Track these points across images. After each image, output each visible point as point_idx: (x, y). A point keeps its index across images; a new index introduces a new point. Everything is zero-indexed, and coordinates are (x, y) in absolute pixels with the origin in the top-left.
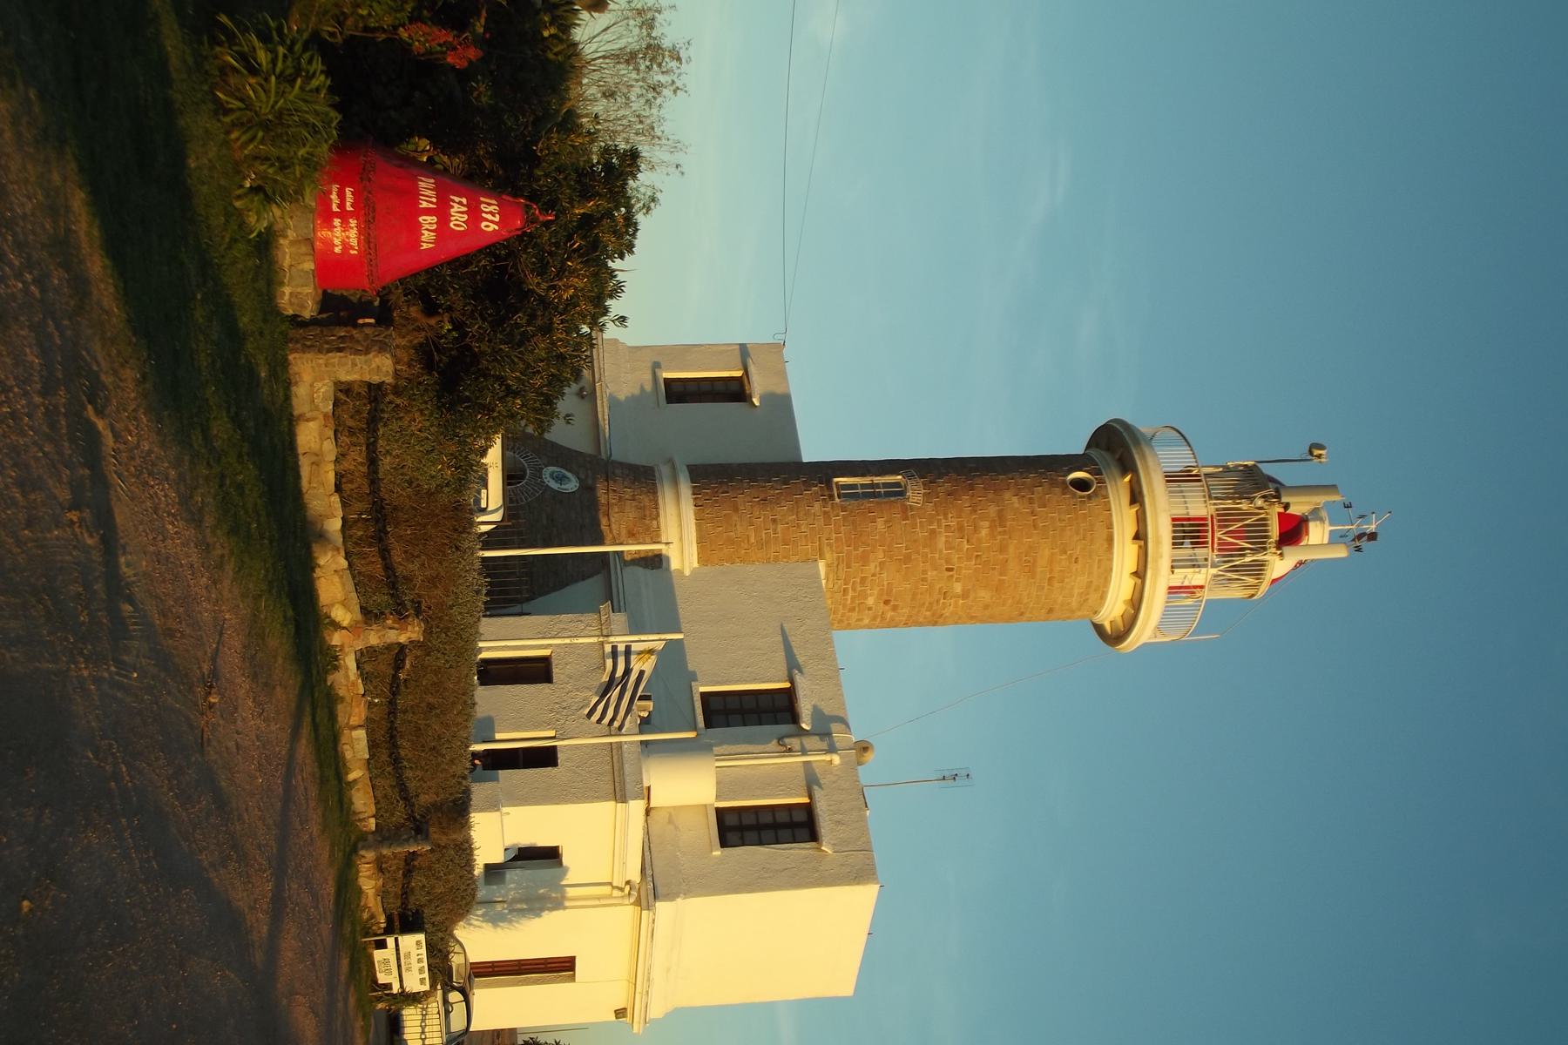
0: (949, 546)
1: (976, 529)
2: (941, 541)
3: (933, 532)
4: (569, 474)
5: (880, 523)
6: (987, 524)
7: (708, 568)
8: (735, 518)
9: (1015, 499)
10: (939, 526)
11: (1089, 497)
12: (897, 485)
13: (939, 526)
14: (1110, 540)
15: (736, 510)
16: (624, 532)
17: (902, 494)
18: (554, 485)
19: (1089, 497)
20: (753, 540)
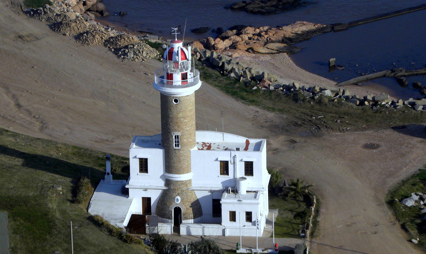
0: (188, 127)
1: (186, 122)
2: (188, 128)
3: (186, 130)
4: (176, 198)
5: (185, 140)
6: (185, 120)
7: (192, 171)
8: (183, 167)
9: (180, 115)
10: (185, 129)
11: (179, 100)
12: (175, 136)
13: (185, 129)
14: (188, 96)
15: (182, 167)
16: (186, 187)
17: (178, 136)
18: (179, 201)
19: (179, 100)
20: (187, 163)
